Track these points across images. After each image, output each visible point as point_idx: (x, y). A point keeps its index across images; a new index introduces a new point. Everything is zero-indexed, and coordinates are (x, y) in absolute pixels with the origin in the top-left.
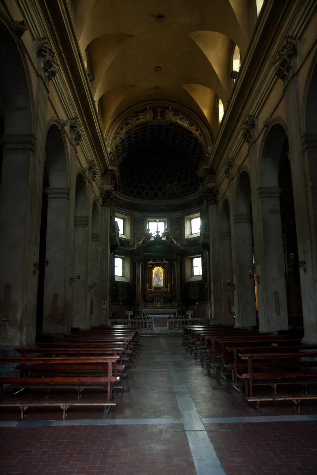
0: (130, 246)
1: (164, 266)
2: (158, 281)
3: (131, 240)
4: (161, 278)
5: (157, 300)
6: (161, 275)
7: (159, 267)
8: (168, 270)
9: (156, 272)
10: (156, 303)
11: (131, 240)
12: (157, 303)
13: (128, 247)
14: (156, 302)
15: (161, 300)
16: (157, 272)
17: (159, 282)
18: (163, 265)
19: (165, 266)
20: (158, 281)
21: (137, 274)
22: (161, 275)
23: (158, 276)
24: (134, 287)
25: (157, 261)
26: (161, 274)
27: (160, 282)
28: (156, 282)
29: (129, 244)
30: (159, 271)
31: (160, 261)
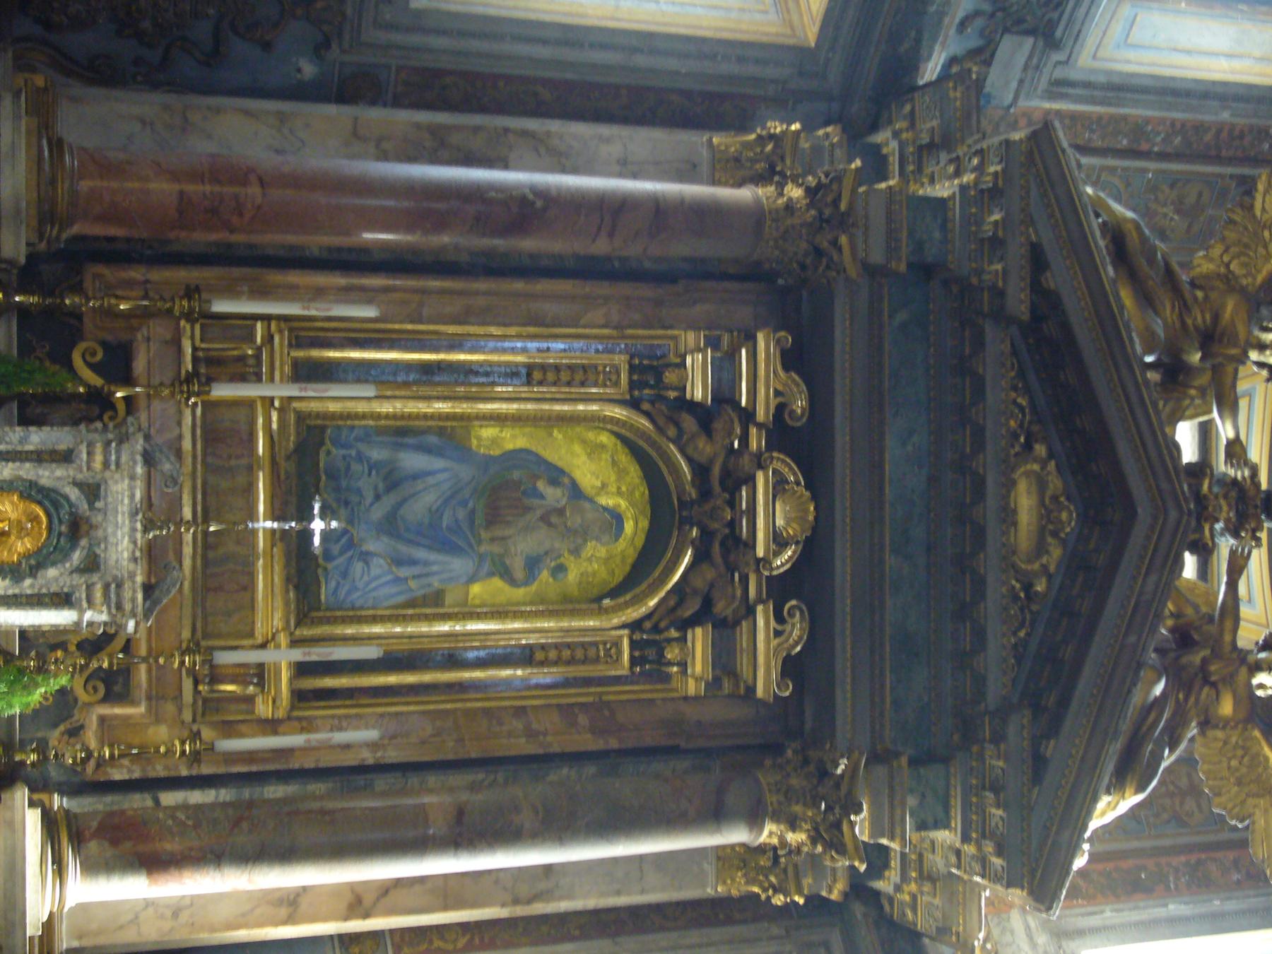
0: (984, 54)
1: (685, 625)
2: (419, 507)
3: (1059, 87)
4: (460, 565)
5: (93, 491)
6: (519, 574)
7: (634, 528)
8: (612, 694)
9: (556, 475)
10: (27, 471)
11: (1059, 87)
12: (32, 492)
13: (963, 25)
14: (48, 475)
15: (92, 565)
16: (553, 495)
17: (391, 526)
18: (721, 607)
19: (699, 639)
20: (419, 507)
21: (555, 126)
22: (506, 574)
23: (493, 519)
24: (309, 70)
25: (779, 486)
26: (533, 565)
27: (399, 562)
28: (393, 480)
29: (1007, 44)
30: (578, 538)
31: (779, 541)
